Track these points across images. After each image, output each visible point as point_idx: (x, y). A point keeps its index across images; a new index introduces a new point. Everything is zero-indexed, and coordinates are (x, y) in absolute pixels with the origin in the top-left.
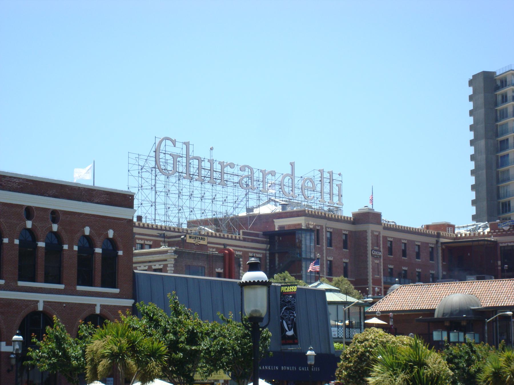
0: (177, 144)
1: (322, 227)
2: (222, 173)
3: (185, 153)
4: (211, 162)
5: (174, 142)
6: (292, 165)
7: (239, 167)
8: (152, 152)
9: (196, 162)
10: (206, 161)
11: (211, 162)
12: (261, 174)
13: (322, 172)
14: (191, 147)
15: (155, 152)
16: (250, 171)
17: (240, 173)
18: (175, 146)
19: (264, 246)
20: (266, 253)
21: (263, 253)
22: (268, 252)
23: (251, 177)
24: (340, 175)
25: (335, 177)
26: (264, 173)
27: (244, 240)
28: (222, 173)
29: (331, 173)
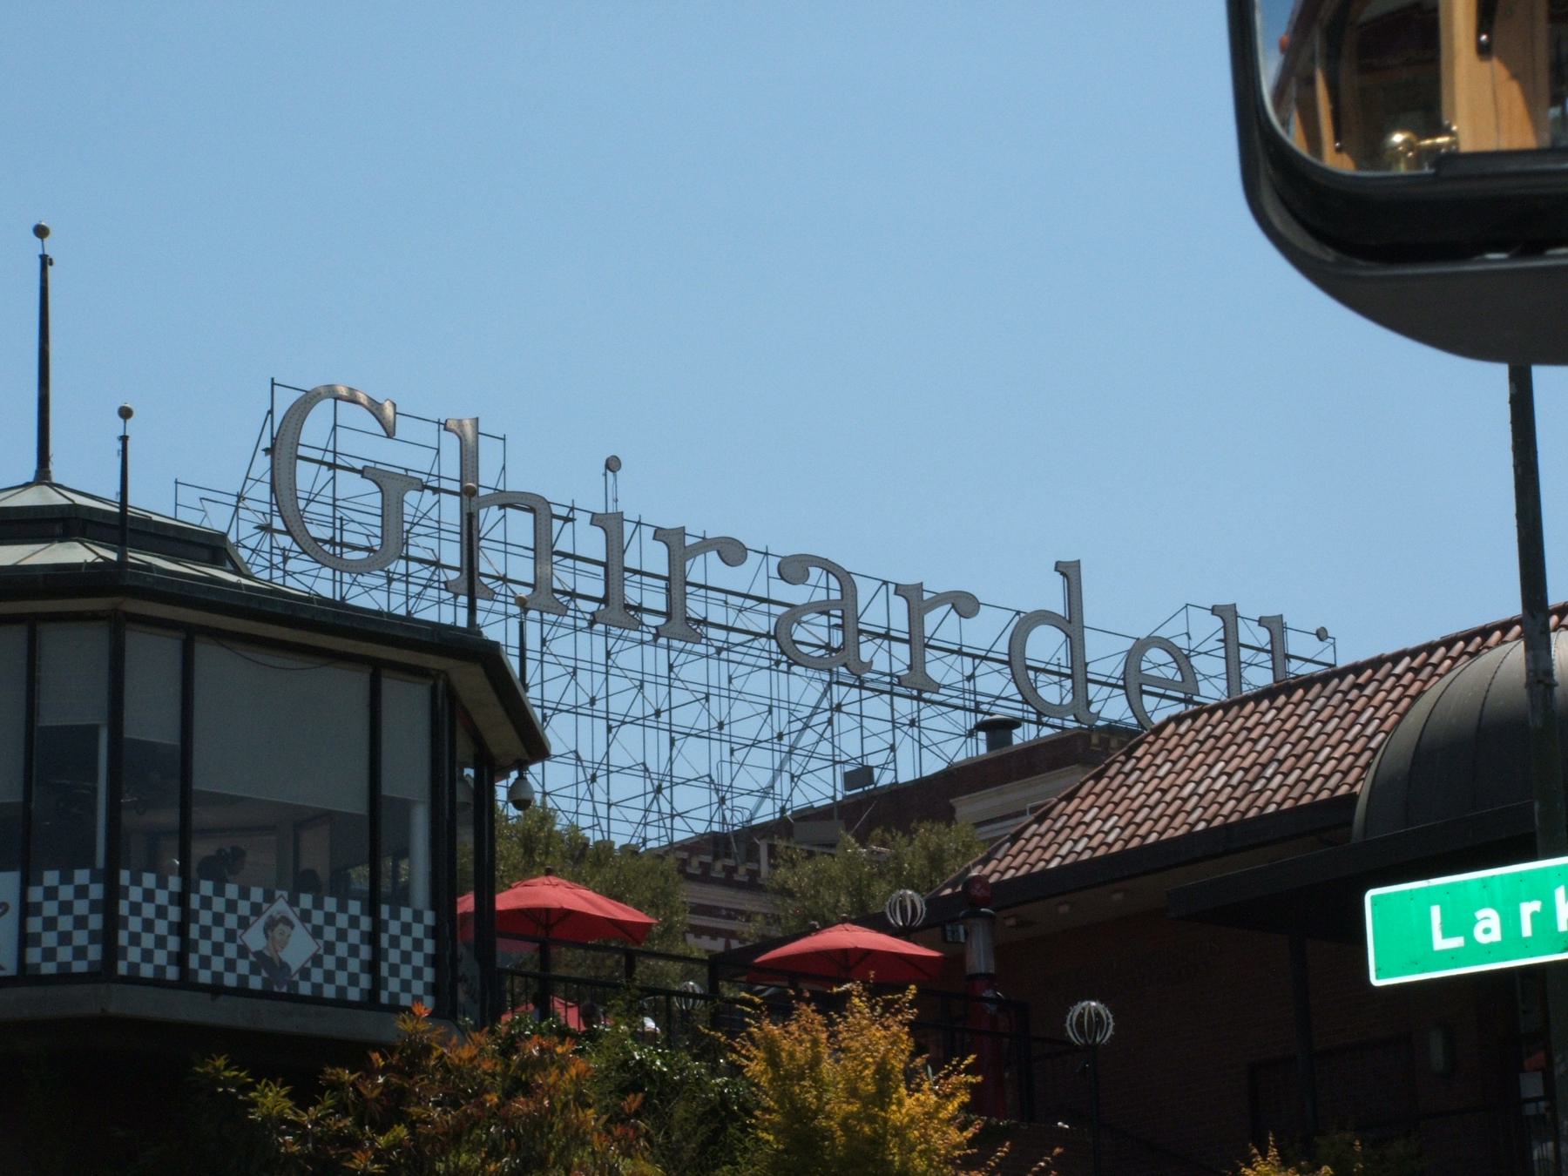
0: (403, 428)
2: (675, 584)
3: (451, 467)
4: (609, 523)
6: (1069, 572)
7: (774, 562)
8: (260, 454)
9: (521, 525)
10: (583, 519)
11: (609, 523)
12: (900, 606)
13: (1227, 615)
15: (270, 451)
16: (834, 583)
18: (390, 434)
23: (844, 609)
24: (1321, 635)
28: (675, 584)
29: (1275, 626)
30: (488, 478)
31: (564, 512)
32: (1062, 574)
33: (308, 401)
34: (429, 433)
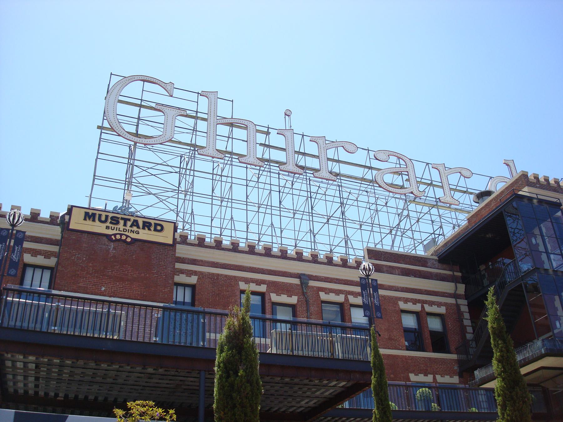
0: (176, 93)
7: (372, 154)
10: (273, 133)
16: (402, 162)
17: (375, 164)
19: (448, 287)
20: (458, 306)
21: (445, 304)
22: (463, 303)
31: (266, 130)
32: (508, 165)
34: (194, 97)
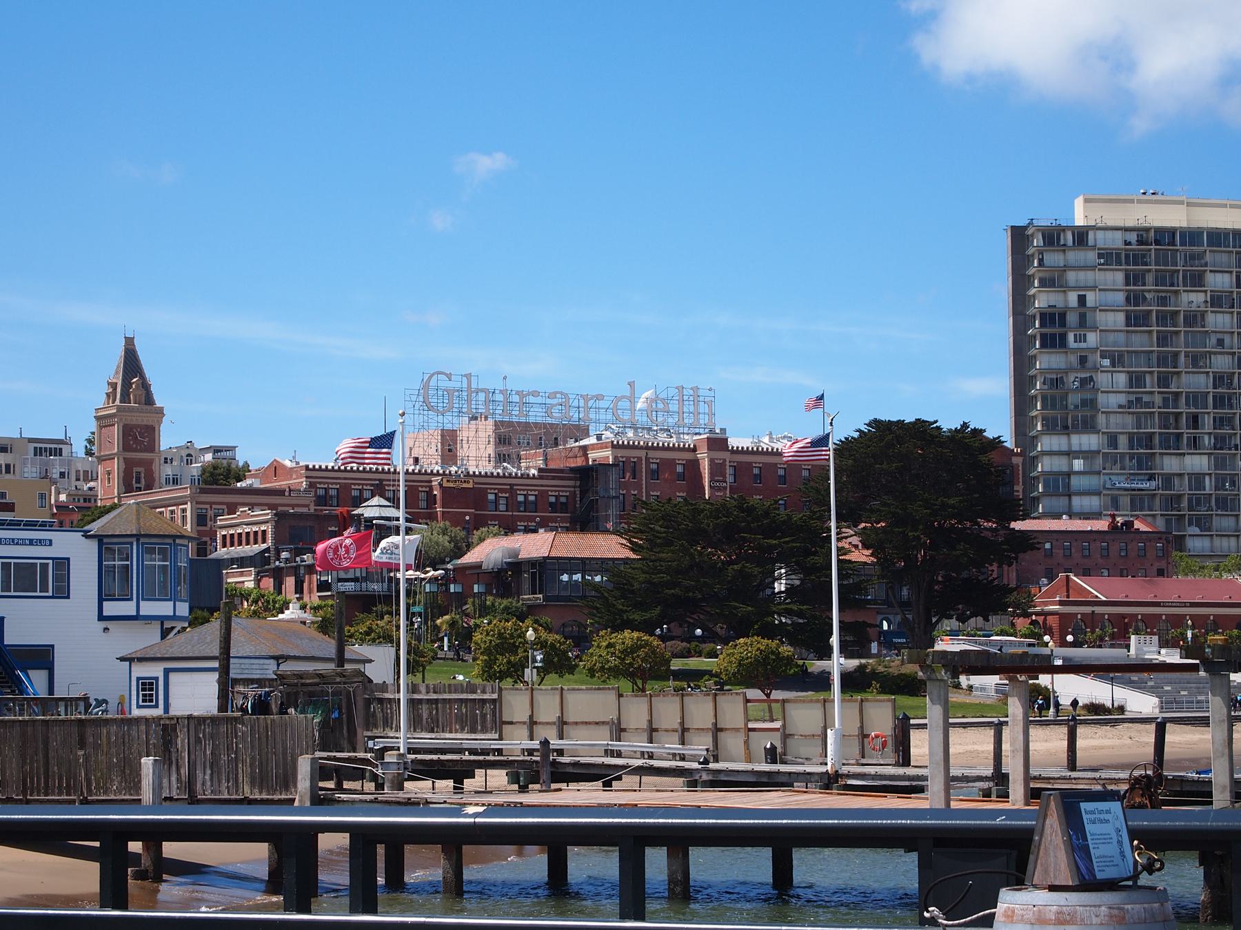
1: (640, 459)
3: (465, 385)
5: (449, 376)
14: (474, 380)
17: (549, 401)
19: (571, 483)
25: (701, 392)
26: (586, 398)
27: (541, 478)
30: (474, 386)
33: (432, 375)
